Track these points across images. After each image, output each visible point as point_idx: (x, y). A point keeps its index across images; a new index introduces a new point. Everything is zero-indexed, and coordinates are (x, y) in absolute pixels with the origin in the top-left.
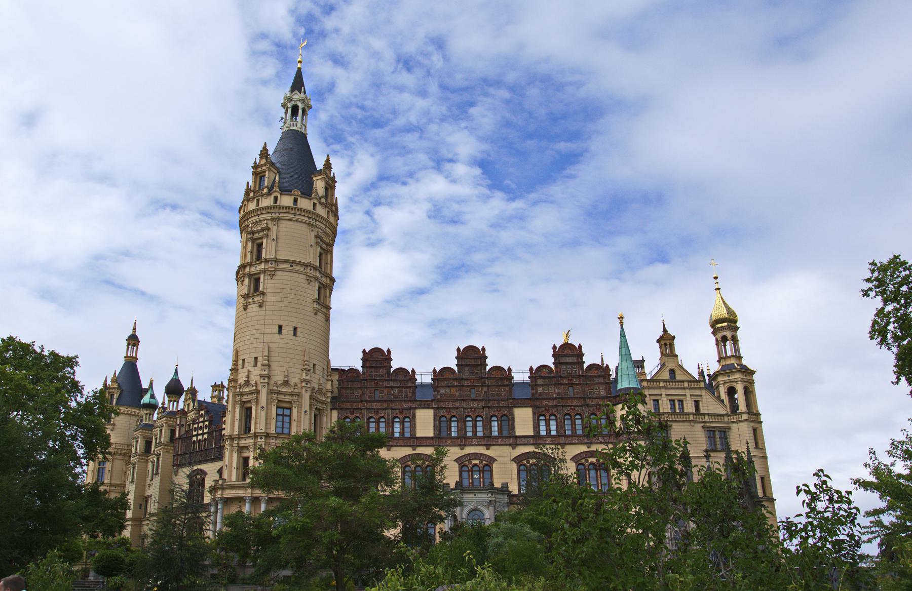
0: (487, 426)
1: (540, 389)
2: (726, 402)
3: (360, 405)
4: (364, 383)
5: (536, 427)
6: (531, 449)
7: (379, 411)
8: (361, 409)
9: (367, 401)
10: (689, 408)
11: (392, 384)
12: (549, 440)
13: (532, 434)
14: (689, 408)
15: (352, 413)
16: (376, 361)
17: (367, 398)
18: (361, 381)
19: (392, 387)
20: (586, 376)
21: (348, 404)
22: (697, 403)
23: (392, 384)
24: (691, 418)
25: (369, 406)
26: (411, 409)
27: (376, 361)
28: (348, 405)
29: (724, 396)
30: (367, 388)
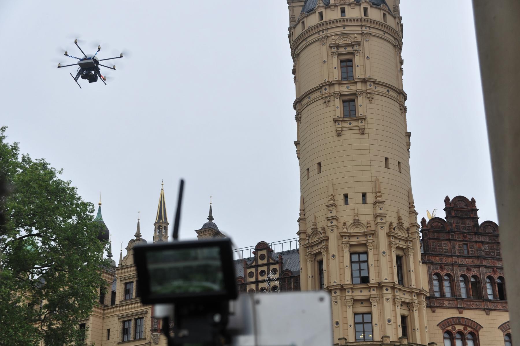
3: (450, 260)
4: (452, 235)
7: (472, 269)
8: (453, 265)
9: (458, 256)
11: (482, 239)
15: (442, 268)
16: (461, 211)
17: (457, 253)
18: (449, 232)
19: (483, 242)
21: (437, 258)
23: (482, 239)
25: (459, 261)
27: (461, 211)
28: (437, 259)
30: (456, 240)
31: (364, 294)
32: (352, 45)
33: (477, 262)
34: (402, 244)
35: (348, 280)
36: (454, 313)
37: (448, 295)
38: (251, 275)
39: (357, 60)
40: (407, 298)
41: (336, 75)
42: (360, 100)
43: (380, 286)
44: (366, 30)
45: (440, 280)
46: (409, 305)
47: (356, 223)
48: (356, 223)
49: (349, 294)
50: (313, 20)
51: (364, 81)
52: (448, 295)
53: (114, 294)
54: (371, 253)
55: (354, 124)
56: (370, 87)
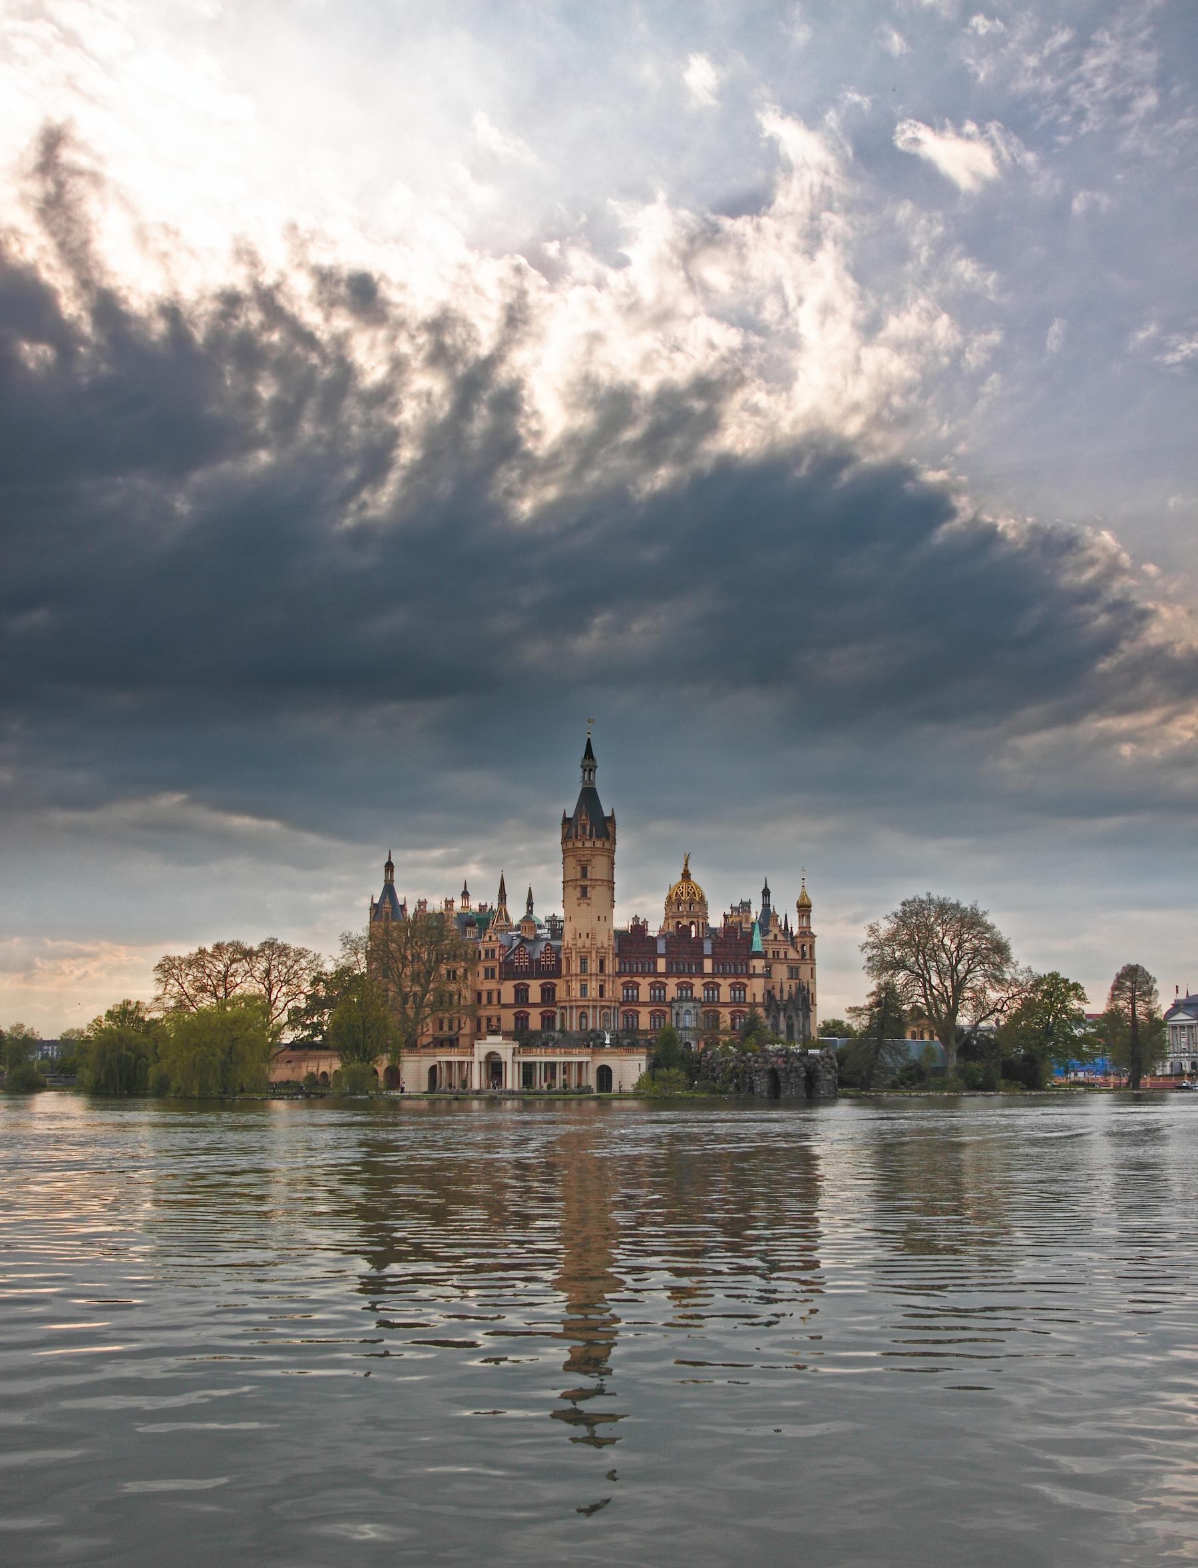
0: (690, 968)
1: (716, 949)
2: (800, 952)
5: (713, 969)
6: (711, 980)
10: (782, 956)
12: (719, 976)
13: (711, 972)
14: (782, 956)
20: (739, 944)
22: (786, 953)
24: (782, 961)
25: (634, 955)
26: (654, 958)
29: (799, 949)
31: (585, 977)
32: (587, 861)
33: (642, 955)
34: (603, 955)
35: (579, 972)
36: (629, 979)
37: (628, 970)
38: (543, 957)
39: (589, 868)
40: (603, 978)
41: (579, 876)
42: (588, 889)
43: (591, 975)
44: (594, 853)
45: (625, 964)
46: (604, 981)
47: (584, 947)
48: (584, 947)
49: (578, 978)
50: (570, 845)
51: (591, 880)
52: (628, 970)
53: (480, 952)
54: (588, 961)
55: (586, 901)
56: (594, 883)
